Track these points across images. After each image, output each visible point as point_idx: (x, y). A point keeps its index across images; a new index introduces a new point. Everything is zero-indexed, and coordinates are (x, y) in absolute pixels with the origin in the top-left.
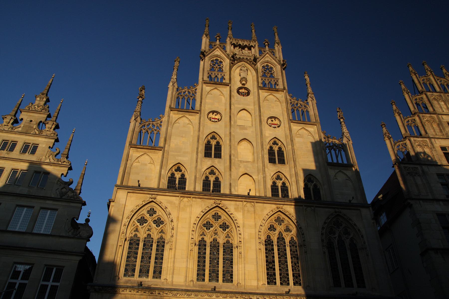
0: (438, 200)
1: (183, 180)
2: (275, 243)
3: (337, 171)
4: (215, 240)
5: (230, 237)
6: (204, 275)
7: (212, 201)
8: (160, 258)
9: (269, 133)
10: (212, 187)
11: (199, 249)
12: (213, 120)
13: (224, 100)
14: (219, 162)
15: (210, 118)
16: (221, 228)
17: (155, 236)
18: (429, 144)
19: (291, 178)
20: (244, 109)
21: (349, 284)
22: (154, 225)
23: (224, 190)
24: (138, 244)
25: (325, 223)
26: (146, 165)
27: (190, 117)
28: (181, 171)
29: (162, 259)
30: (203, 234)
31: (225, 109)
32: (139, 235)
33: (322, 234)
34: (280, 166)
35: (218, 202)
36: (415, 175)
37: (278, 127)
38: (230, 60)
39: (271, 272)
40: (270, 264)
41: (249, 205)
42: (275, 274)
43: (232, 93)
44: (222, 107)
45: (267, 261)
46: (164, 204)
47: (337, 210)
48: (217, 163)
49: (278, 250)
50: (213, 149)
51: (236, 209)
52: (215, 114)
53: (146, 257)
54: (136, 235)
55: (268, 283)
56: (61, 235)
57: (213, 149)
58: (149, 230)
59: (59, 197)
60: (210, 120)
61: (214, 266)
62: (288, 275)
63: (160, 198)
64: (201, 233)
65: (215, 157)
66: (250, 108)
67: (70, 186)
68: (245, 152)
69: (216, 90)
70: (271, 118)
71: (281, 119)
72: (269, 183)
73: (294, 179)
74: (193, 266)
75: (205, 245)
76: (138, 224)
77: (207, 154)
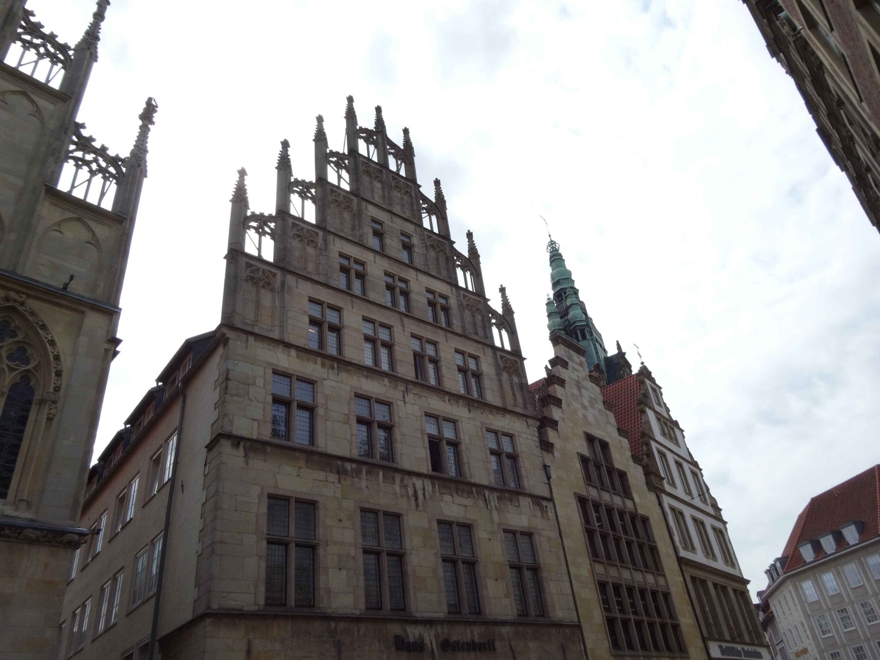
0: (288, 346)
3: (69, 215)
36: (263, 287)
47: (13, 295)
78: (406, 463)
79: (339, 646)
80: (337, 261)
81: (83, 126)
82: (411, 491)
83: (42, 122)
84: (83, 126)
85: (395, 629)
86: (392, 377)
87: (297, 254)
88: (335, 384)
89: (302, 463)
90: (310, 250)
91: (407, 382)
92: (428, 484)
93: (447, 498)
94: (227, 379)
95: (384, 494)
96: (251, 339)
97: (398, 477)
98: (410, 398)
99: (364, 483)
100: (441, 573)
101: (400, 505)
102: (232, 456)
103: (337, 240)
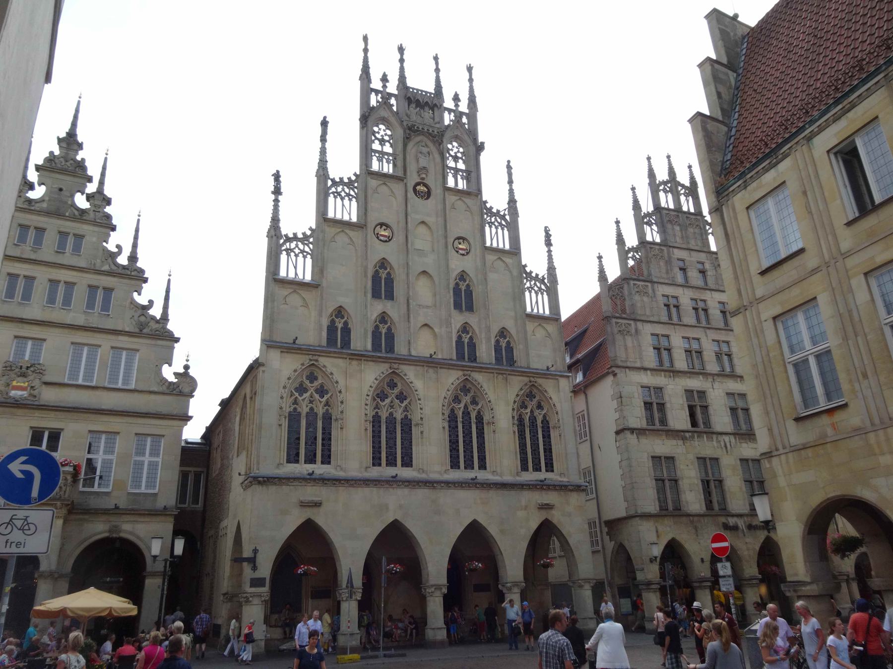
0: (646, 369)
2: (460, 419)
4: (391, 414)
6: (380, 459)
9: (457, 264)
11: (373, 426)
12: (382, 238)
17: (320, 410)
18: (650, 291)
20: (423, 222)
22: (317, 396)
23: (401, 349)
24: (299, 421)
25: (517, 395)
29: (330, 439)
31: (398, 222)
32: (299, 410)
33: (513, 409)
34: (467, 314)
35: (396, 366)
37: (467, 253)
38: (405, 132)
40: (453, 444)
41: (431, 370)
42: (458, 457)
45: (450, 441)
46: (330, 369)
47: (532, 379)
52: (384, 227)
54: (295, 409)
55: (452, 467)
56: (151, 389)
57: (382, 284)
58: (311, 402)
59: (137, 330)
62: (472, 457)
63: (323, 361)
66: (431, 220)
67: (151, 312)
68: (423, 291)
69: (384, 187)
70: (459, 238)
71: (471, 241)
73: (483, 335)
74: (367, 448)
75: (380, 422)
76: (297, 394)
77: (376, 294)
78: (718, 428)
79: (696, 528)
80: (662, 301)
81: (525, 266)
82: (723, 444)
83: (510, 272)
85: (723, 520)
86: (706, 375)
87: (639, 305)
88: (672, 387)
89: (664, 437)
90: (645, 299)
91: (713, 375)
92: (732, 438)
93: (744, 445)
94: (621, 397)
95: (708, 448)
96: (627, 370)
97: (714, 436)
98: (716, 385)
99: (697, 443)
100: (744, 489)
101: (717, 453)
102: (632, 439)
103: (660, 286)
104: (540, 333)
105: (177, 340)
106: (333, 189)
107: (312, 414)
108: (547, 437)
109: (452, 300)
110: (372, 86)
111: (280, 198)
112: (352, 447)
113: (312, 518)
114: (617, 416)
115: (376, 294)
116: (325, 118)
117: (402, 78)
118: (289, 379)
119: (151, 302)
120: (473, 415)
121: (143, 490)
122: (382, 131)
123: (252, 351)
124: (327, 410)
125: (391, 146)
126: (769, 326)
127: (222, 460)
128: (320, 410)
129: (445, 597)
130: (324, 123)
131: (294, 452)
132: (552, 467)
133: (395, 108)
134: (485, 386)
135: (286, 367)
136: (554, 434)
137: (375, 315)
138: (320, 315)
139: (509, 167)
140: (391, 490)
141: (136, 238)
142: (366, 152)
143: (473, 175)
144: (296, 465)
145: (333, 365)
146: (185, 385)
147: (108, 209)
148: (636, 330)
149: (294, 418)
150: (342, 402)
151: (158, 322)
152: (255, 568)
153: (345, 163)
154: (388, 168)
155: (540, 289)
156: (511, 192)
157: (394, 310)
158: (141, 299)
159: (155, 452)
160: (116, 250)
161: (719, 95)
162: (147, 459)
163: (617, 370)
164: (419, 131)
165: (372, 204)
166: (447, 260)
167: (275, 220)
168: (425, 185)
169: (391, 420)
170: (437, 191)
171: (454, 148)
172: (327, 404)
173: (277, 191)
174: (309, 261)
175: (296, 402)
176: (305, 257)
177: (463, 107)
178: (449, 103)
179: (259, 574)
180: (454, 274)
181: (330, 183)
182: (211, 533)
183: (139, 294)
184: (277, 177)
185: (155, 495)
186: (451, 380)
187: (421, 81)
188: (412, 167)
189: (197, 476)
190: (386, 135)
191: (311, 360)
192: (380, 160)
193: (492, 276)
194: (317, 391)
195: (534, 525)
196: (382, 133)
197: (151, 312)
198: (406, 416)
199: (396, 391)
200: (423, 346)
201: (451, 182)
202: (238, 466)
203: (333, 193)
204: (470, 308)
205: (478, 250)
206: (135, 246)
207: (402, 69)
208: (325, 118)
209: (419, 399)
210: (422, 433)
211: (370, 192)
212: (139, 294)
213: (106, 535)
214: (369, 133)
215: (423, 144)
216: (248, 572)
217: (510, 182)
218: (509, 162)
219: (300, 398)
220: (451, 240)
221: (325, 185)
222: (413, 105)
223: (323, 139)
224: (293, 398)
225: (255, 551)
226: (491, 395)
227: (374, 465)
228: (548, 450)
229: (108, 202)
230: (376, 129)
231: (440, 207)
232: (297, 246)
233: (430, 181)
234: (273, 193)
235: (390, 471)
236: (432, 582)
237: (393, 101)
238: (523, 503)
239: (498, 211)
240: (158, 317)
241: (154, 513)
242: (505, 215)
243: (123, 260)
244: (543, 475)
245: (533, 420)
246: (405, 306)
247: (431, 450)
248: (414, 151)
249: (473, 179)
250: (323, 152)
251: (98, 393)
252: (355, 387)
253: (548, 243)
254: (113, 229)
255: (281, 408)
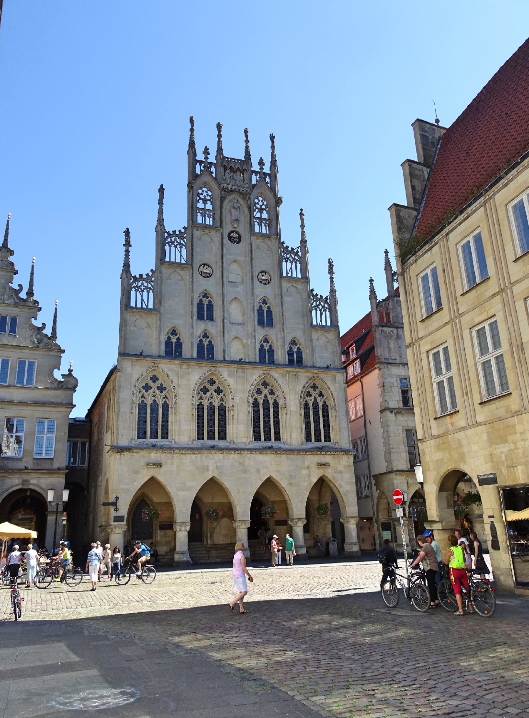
1: (179, 345)
2: (261, 406)
4: (211, 403)
5: (223, 401)
7: (208, 368)
8: (165, 421)
9: (261, 291)
10: (206, 352)
11: (198, 411)
13: (216, 247)
14: (212, 326)
15: (201, 272)
16: (215, 392)
17: (160, 402)
19: (277, 341)
20: (235, 261)
21: (318, 439)
22: (158, 392)
23: (218, 355)
24: (146, 410)
25: (304, 387)
26: (143, 329)
27: (182, 273)
28: (176, 334)
30: (201, 398)
31: (217, 262)
33: (301, 397)
34: (267, 329)
35: (214, 369)
37: (269, 283)
38: (221, 192)
39: (257, 429)
43: (224, 241)
44: (212, 258)
48: (210, 326)
49: (263, 411)
50: (205, 311)
51: (229, 375)
52: (206, 266)
53: (154, 421)
54: (143, 401)
57: (205, 311)
58: (154, 396)
60: (201, 275)
61: (211, 426)
62: (270, 432)
64: (199, 397)
65: (207, 319)
67: (44, 332)
68: (235, 312)
69: (206, 236)
70: (262, 272)
71: (272, 274)
72: (258, 347)
74: (194, 427)
75: (203, 408)
76: (144, 391)
77: (200, 317)
84: (313, 290)
94: (384, 386)
102: (391, 417)
104: (323, 340)
105: (63, 351)
106: (169, 240)
107: (155, 405)
108: (326, 416)
109: (256, 318)
110: (197, 158)
111: (130, 249)
112: (183, 425)
113: (155, 476)
114: (381, 400)
115: (200, 317)
116: (162, 186)
117: (220, 150)
118: (138, 380)
119: (44, 325)
120: (271, 402)
121: (44, 456)
122: (204, 192)
123: (113, 360)
124: (165, 402)
125: (212, 204)
126: (424, 356)
127: (98, 434)
128: (160, 402)
129: (249, 529)
130: (161, 190)
131: (142, 432)
132: (330, 438)
133: (214, 175)
134: (280, 381)
135: (136, 372)
136: (331, 415)
137: (200, 332)
138: (160, 334)
139: (301, 214)
140: (210, 456)
141: (31, 280)
142: (193, 210)
143: (274, 222)
144: (144, 440)
145: (168, 368)
146: (70, 384)
147: (11, 259)
148: (397, 335)
149: (142, 407)
150: (176, 396)
151: (49, 338)
152: (116, 510)
153: (177, 220)
154: (209, 221)
155: (323, 307)
156: (303, 233)
157: (213, 329)
158: (37, 323)
159: (50, 431)
160: (18, 288)
161: (413, 188)
162: (45, 436)
163: (381, 366)
164: (234, 190)
165: (197, 250)
166: (253, 289)
167: (127, 266)
168: (238, 233)
169: (211, 408)
170: (245, 236)
171: (260, 202)
172: (165, 397)
173: (128, 244)
174: (151, 294)
175: (143, 396)
176: (148, 292)
177: (267, 169)
178: (256, 167)
179: (119, 514)
180: (258, 299)
181: (166, 235)
182: (93, 484)
183: (36, 319)
184: (127, 233)
185: (52, 459)
186: (255, 377)
187: (234, 151)
188: (227, 219)
189: (83, 445)
190: (208, 195)
191: (153, 367)
192: (203, 216)
193: (286, 299)
194: (158, 388)
195: (315, 480)
196: (205, 194)
197: (44, 332)
198: (222, 404)
199: (215, 387)
200: (236, 351)
201: (257, 229)
202: (108, 439)
203: (168, 243)
204: (270, 324)
205: (276, 280)
206: (31, 285)
207: (219, 142)
208: (162, 186)
209: (231, 392)
210: (233, 416)
211: (195, 240)
212: (36, 319)
213: (20, 487)
214: (195, 196)
215: (236, 201)
216: (113, 513)
217: (303, 226)
218: (302, 210)
219: (146, 394)
220: (256, 273)
221: (163, 238)
222: (228, 171)
223: (161, 202)
224: (141, 393)
225: (117, 498)
226: (285, 389)
227: (199, 439)
228: (327, 426)
229: (11, 253)
230: (200, 191)
231: (248, 248)
232: (142, 284)
233: (241, 230)
234: (124, 245)
235: (211, 443)
236: (238, 519)
237: (213, 169)
238: (307, 464)
239: (292, 249)
240: (49, 335)
241: (51, 472)
242: (298, 252)
243: (23, 295)
244: (323, 443)
245: (315, 404)
246: (222, 324)
247: (240, 428)
248: (228, 206)
249: (274, 226)
250: (161, 211)
251: (11, 390)
252: (184, 383)
253: (331, 271)
254: (16, 273)
255: (133, 401)
